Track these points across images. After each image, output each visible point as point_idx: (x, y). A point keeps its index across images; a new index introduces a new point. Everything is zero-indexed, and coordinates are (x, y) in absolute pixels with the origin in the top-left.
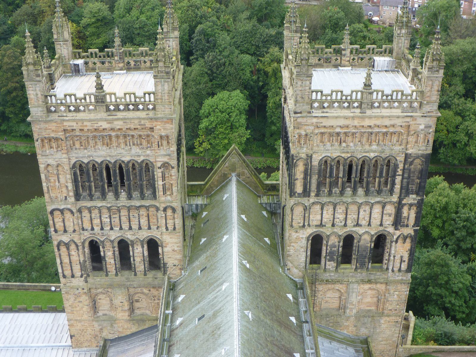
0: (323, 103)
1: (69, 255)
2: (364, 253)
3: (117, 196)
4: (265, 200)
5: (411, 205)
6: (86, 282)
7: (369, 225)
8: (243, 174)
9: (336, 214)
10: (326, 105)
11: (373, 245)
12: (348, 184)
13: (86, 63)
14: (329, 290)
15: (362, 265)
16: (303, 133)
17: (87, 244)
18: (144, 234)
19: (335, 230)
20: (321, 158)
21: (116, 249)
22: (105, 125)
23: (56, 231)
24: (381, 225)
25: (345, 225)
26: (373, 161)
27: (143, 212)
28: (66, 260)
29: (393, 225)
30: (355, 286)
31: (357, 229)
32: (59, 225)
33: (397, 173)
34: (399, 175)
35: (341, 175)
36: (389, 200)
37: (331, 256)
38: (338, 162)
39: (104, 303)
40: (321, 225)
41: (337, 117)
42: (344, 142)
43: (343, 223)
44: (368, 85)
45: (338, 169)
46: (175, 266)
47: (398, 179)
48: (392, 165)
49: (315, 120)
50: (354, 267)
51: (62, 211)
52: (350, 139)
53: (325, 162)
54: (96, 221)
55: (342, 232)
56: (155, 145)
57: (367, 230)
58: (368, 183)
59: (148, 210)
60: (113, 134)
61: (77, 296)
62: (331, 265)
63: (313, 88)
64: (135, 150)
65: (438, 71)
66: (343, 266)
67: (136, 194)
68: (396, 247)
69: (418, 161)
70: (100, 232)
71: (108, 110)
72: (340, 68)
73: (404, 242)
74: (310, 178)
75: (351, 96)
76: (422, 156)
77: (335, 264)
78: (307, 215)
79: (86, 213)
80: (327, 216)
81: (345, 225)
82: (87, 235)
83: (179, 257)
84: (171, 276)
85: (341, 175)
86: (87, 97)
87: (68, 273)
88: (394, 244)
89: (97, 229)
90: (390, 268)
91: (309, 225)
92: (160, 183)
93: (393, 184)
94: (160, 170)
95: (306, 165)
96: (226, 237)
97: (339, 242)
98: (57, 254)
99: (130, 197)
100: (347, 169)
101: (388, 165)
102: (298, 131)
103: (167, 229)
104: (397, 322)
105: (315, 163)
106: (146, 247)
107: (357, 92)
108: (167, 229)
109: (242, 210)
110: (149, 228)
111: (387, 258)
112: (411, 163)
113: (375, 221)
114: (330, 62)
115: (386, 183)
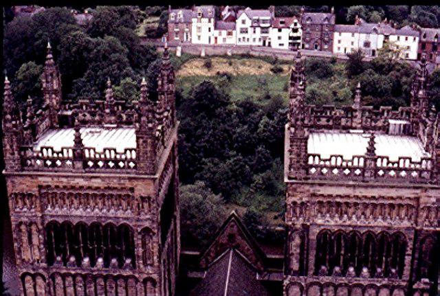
34: (409, 255)
42: (346, 213)
44: (371, 150)
52: (351, 211)
53: (324, 234)
71: (85, 166)
72: (351, 131)
74: (308, 254)
79: (59, 280)
86: (65, 151)
92: (140, 251)
93: (402, 266)
94: (140, 237)
105: (313, 237)
107: (359, 157)
112: (423, 241)
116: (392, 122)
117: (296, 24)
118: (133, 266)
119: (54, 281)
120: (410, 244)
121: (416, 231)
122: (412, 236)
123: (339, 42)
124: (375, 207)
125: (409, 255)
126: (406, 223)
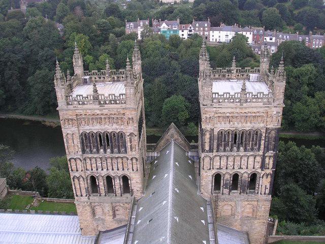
1: (79, 184)
3: (105, 151)
5: (270, 157)
6: (89, 199)
7: (247, 168)
10: (221, 101)
11: (249, 179)
12: (234, 145)
13: (91, 78)
15: (243, 191)
17: (89, 178)
18: (121, 173)
19: (228, 171)
21: (105, 181)
22: (98, 112)
23: (72, 170)
25: (234, 168)
26: (248, 132)
27: (120, 160)
28: (78, 187)
32: (74, 167)
35: (230, 140)
37: (226, 186)
38: (229, 132)
39: (99, 211)
40: (220, 168)
41: (227, 108)
45: (229, 136)
47: (263, 142)
49: (214, 109)
51: (75, 159)
54: (94, 165)
55: (232, 172)
56: (126, 123)
58: (246, 145)
59: (122, 160)
60: (103, 117)
61: (84, 207)
62: (226, 191)
64: (115, 126)
65: (282, 81)
66: (233, 191)
67: (116, 150)
69: (273, 132)
70: (96, 171)
73: (267, 178)
74: (213, 142)
75: (235, 96)
79: (88, 161)
80: (223, 163)
81: (234, 168)
82: (89, 173)
83: (140, 186)
84: (136, 196)
87: (79, 194)
89: (94, 169)
90: (260, 192)
91: (213, 168)
92: (128, 144)
93: (260, 145)
94: (128, 137)
96: (166, 175)
98: (73, 183)
99: (112, 152)
101: (257, 134)
102: (205, 115)
103: (133, 170)
105: (216, 133)
106: (121, 180)
108: (133, 170)
109: (175, 160)
110: (123, 170)
112: (269, 133)
113: (250, 166)
115: (256, 145)
116: (251, 75)
117: (190, 28)
118: (126, 152)
119: (85, 160)
120: (264, 135)
121: (266, 128)
122: (265, 131)
123: (213, 36)
124: (246, 118)
126: (262, 125)
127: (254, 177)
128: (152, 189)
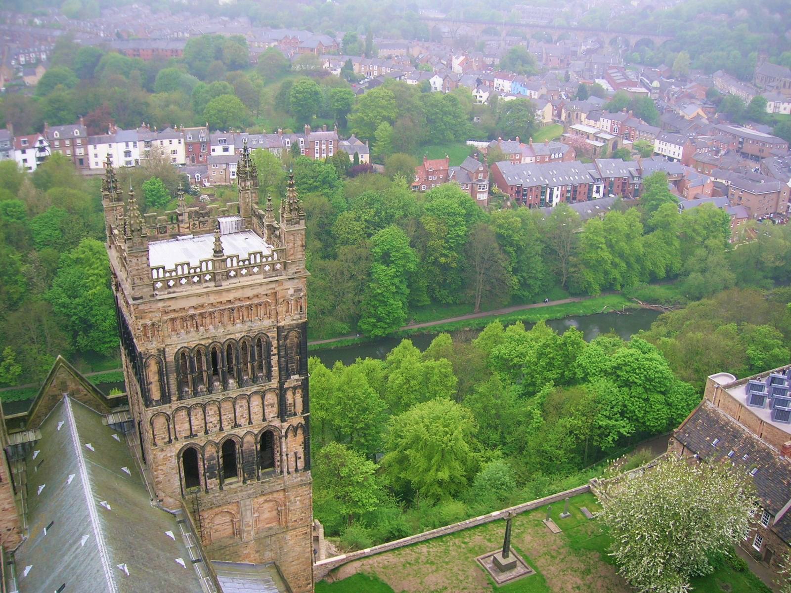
0: (168, 281)
2: (251, 459)
4: (112, 419)
7: (250, 422)
8: (78, 391)
9: (208, 418)
10: (171, 283)
11: (259, 447)
12: (214, 378)
14: (217, 514)
16: (149, 323)
19: (211, 438)
20: (176, 350)
24: (264, 420)
25: (221, 429)
26: (241, 344)
29: (278, 417)
30: (248, 502)
31: (236, 431)
33: (272, 353)
34: (274, 355)
35: (205, 368)
36: (267, 387)
38: (198, 351)
40: (192, 435)
41: (188, 296)
42: (202, 325)
43: (218, 427)
44: (218, 251)
45: (199, 361)
46: (9, 530)
47: (274, 359)
48: (264, 343)
49: (160, 304)
50: (242, 479)
52: (208, 320)
53: (182, 355)
57: (248, 429)
58: (239, 372)
62: (213, 483)
63: (152, 265)
65: (298, 223)
66: (227, 481)
68: (287, 443)
69: (293, 334)
72: (179, 238)
73: (295, 436)
76: (298, 326)
77: (218, 481)
78: (171, 426)
81: (221, 429)
85: (205, 368)
88: (284, 438)
90: (285, 470)
91: (176, 439)
93: (270, 367)
95: (159, 363)
97: (218, 452)
100: (210, 359)
101: (259, 345)
102: (142, 322)
104: (306, 533)
105: (170, 358)
107: (207, 261)
109: (84, 439)
111: (279, 458)
112: (286, 338)
113: (257, 418)
114: (166, 232)
115: (260, 368)
117: (41, 142)
121: (278, 328)
122: (275, 335)
123: (96, 156)
124: (232, 311)
125: (274, 355)
126: (267, 323)
127: (267, 439)
128: (43, 518)
